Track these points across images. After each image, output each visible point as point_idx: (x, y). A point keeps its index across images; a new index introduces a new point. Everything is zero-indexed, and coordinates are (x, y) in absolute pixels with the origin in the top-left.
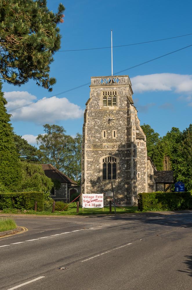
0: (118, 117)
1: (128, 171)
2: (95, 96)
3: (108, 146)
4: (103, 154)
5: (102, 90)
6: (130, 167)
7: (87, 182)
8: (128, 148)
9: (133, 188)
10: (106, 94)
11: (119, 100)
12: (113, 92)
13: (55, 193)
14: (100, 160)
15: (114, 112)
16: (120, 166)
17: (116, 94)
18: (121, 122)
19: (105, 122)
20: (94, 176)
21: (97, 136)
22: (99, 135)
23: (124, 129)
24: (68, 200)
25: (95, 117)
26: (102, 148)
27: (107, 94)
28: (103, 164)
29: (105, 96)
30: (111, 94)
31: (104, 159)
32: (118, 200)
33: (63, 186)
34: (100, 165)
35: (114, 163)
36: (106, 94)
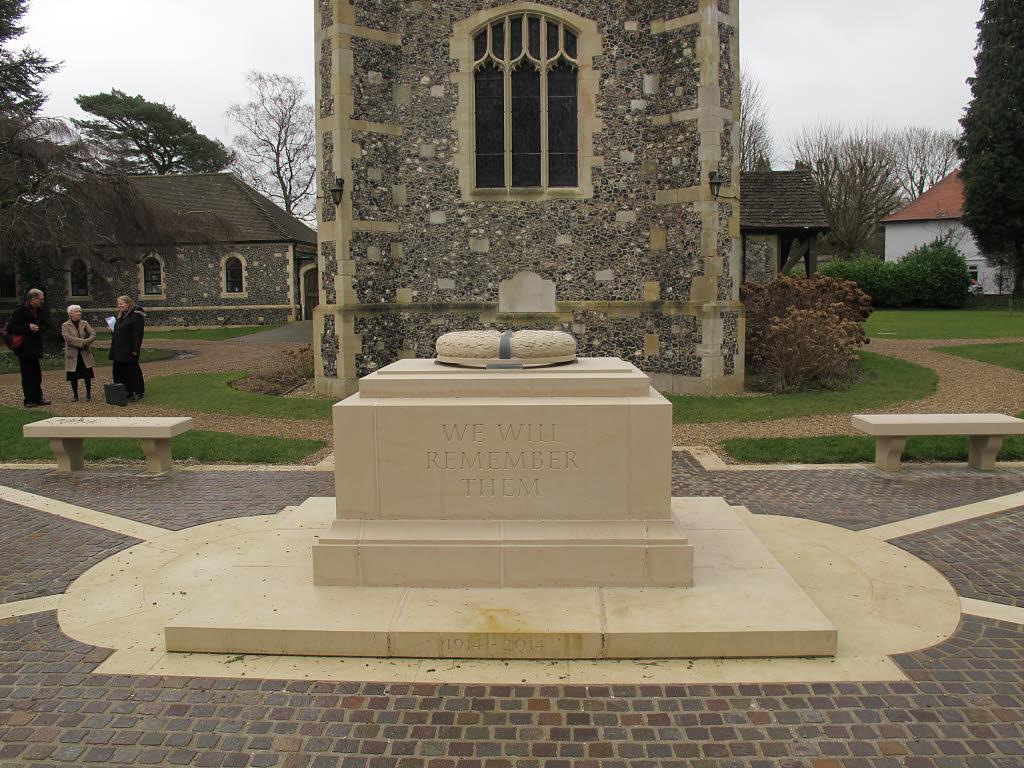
6: (691, 92)
13: (245, 284)
14: (452, 41)
16: (610, 82)
20: (408, 160)
28: (477, 74)
31: (484, 33)
32: (596, 343)
33: (276, 255)
34: (454, 78)
35: (561, 61)
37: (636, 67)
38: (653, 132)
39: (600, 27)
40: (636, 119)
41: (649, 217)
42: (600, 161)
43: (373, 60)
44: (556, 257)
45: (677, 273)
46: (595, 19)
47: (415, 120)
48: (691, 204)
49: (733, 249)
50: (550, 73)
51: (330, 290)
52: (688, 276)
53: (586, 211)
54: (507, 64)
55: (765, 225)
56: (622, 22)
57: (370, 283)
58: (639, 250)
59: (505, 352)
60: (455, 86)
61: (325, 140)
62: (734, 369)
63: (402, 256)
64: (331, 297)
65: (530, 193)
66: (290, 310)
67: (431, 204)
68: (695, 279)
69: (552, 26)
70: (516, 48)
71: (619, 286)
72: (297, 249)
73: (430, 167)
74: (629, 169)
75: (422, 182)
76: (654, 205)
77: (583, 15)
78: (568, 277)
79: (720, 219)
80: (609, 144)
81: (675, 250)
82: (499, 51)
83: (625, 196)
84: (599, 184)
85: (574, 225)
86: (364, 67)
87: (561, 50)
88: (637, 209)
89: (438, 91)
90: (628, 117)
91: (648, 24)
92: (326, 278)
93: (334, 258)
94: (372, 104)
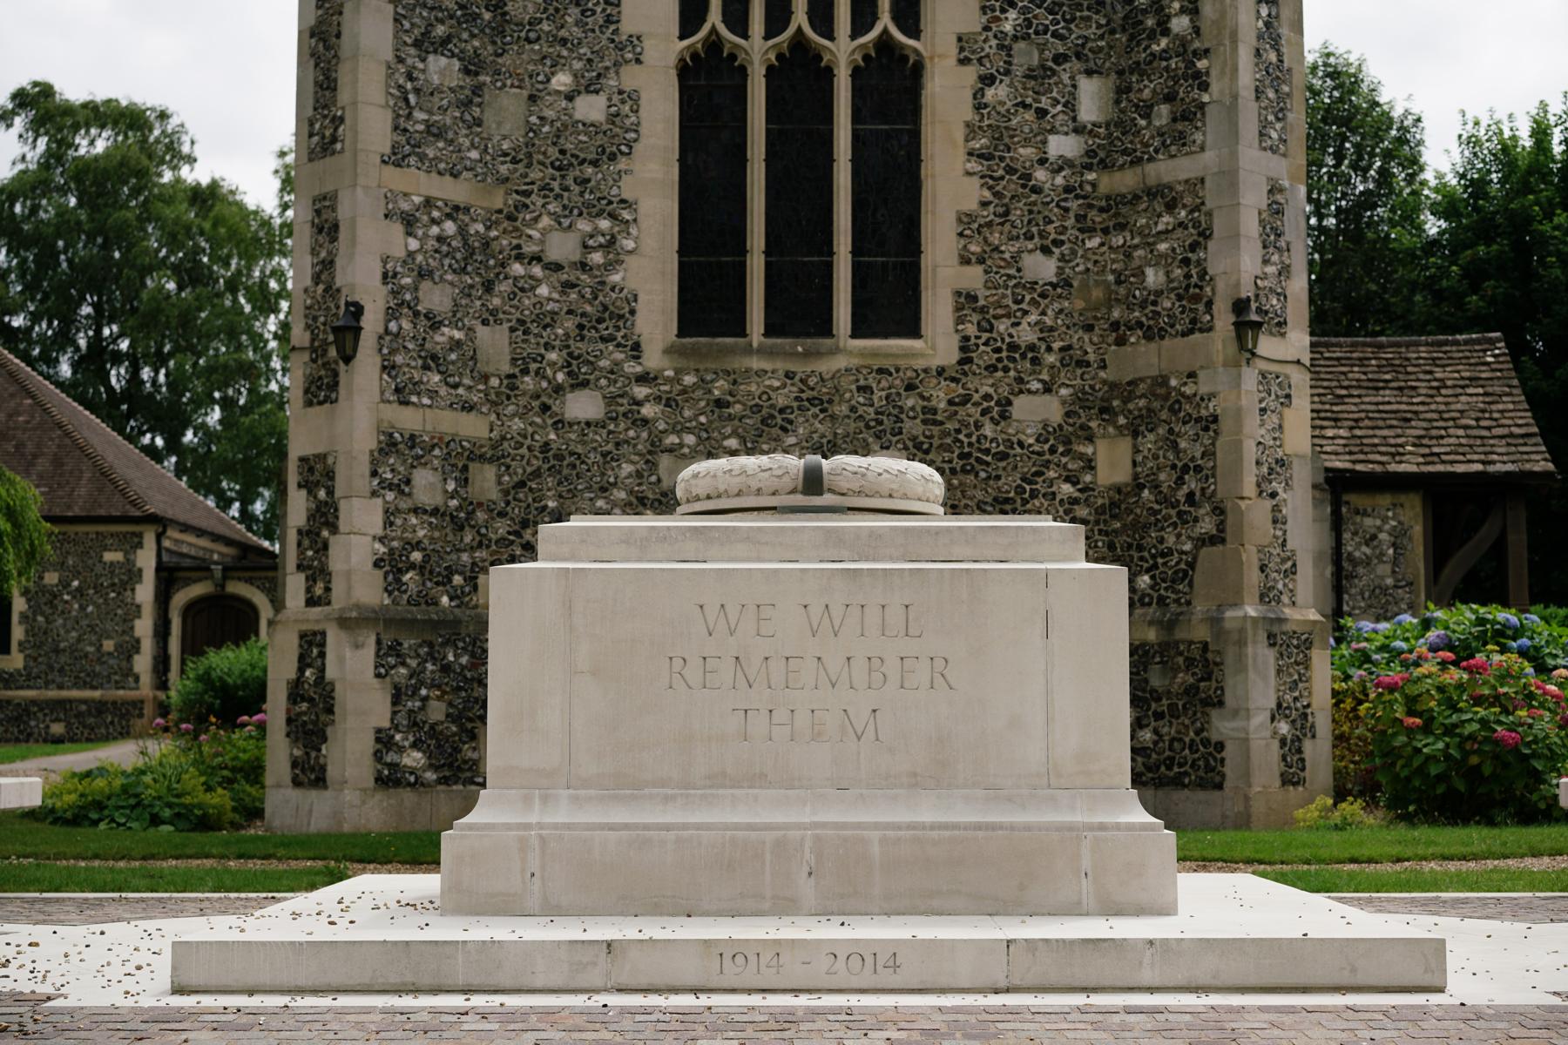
1: (1153, 192)
6: (1190, 115)
7: (388, 368)
9: (1249, 489)
13: (18, 633)
20: (517, 268)
33: (109, 556)
34: (631, 78)
35: (884, 41)
37: (1060, 59)
38: (1102, 210)
40: (1059, 180)
42: (973, 278)
43: (440, 30)
45: (1161, 540)
47: (535, 174)
48: (1192, 375)
49: (1295, 483)
50: (856, 73)
51: (317, 573)
52: (1187, 547)
53: (940, 395)
55: (1393, 467)
57: (416, 556)
58: (1067, 488)
59: (813, 482)
60: (632, 98)
61: (318, 212)
62: (1307, 773)
63: (494, 494)
64: (319, 590)
65: (807, 355)
66: (138, 704)
67: (569, 374)
68: (1204, 551)
72: (166, 543)
73: (569, 285)
74: (1043, 295)
75: (547, 320)
76: (1104, 382)
79: (1263, 411)
80: (995, 238)
81: (1156, 487)
83: (1035, 361)
84: (971, 330)
85: (913, 427)
86: (417, 44)
87: (885, 21)
88: (1063, 391)
89: (591, 108)
90: (1041, 175)
92: (306, 542)
93: (330, 492)
94: (435, 132)
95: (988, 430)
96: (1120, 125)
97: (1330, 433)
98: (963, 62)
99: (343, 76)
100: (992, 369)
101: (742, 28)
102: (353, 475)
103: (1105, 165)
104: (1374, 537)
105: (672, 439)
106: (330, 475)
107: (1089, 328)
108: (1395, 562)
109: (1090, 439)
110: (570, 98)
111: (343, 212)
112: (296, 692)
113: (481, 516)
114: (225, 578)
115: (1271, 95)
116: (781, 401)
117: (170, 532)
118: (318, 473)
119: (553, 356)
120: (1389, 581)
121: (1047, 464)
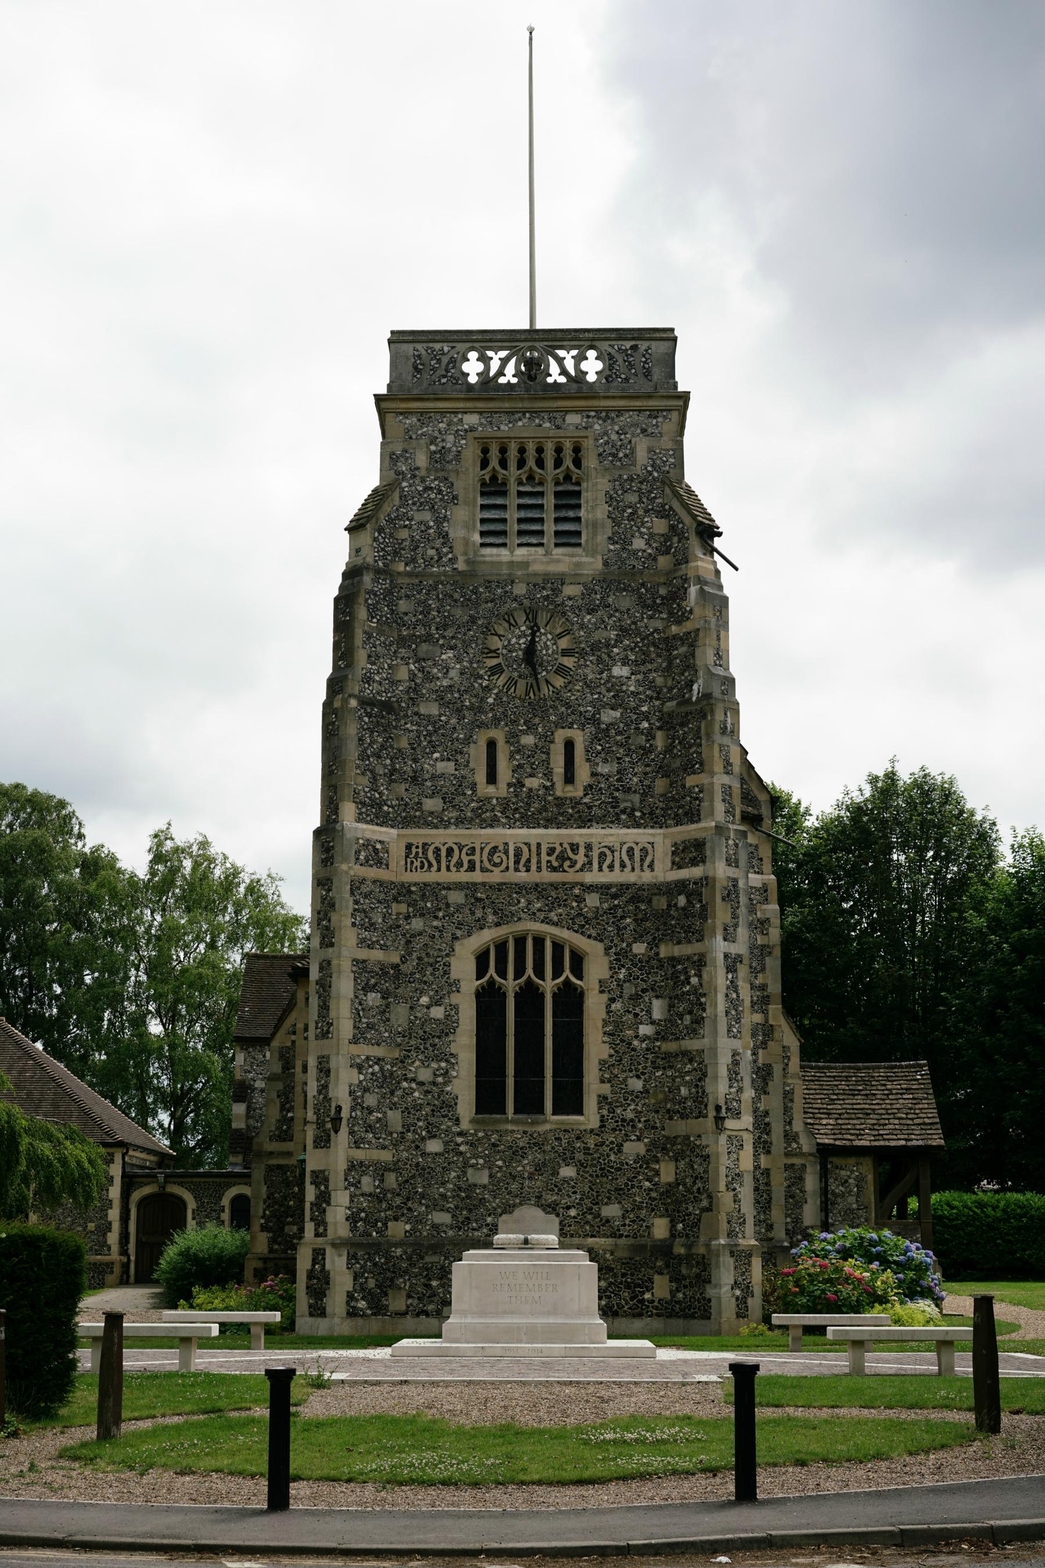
0: (600, 635)
1: (685, 1053)
2: (423, 473)
3: (518, 854)
4: (479, 914)
5: (472, 429)
6: (699, 1021)
7: (352, 1133)
8: (677, 865)
9: (722, 1187)
10: (503, 464)
11: (602, 512)
12: (559, 450)
14: (453, 960)
15: (570, 590)
17: (577, 463)
18: (620, 671)
19: (497, 670)
20: (405, 1084)
21: (434, 777)
22: (448, 767)
23: (646, 725)
24: (126, 1266)
25: (420, 631)
26: (472, 868)
27: (512, 464)
29: (494, 478)
30: (540, 463)
34: (455, 999)
35: (567, 982)
36: (503, 464)
37: (644, 991)
38: (662, 1059)
39: (607, 949)
40: (644, 1045)
41: (661, 1147)
42: (606, 1088)
43: (373, 981)
44: (560, 1190)
45: (687, 1209)
46: (601, 941)
47: (412, 1042)
48: (699, 1136)
49: (745, 1184)
51: (320, 1223)
52: (697, 1212)
53: (591, 1142)
54: (511, 985)
55: (855, 1143)
56: (629, 945)
57: (363, 1215)
58: (647, 1184)
59: (526, 1241)
60: (456, 1008)
61: (320, 1063)
62: (749, 1313)
63: (395, 1186)
64: (321, 1230)
65: (533, 1123)
66: (110, 1265)
67: (428, 1132)
68: (704, 1214)
69: (558, 948)
70: (519, 972)
71: (627, 1222)
73: (427, 1092)
74: (637, 1097)
75: (418, 1108)
76: (664, 1136)
77: (589, 937)
78: (573, 1212)
79: (729, 1153)
80: (616, 1071)
81: (685, 1185)
82: (502, 973)
83: (633, 1126)
84: (605, 1112)
85: (579, 1156)
86: (363, 989)
87: (567, 973)
88: (646, 1140)
89: (438, 1012)
90: (636, 1043)
91: (657, 946)
92: (315, 1209)
93: (327, 1187)
94: (370, 1027)
95: (612, 1157)
96: (670, 1022)
97: (824, 1122)
98: (602, 992)
99: (332, 1004)
100: (614, 1130)
101: (502, 974)
102: (337, 1180)
103: (664, 1039)
104: (846, 1181)
105: (473, 1161)
106: (327, 1180)
107: (657, 1112)
108: (858, 1195)
109: (658, 1162)
110: (428, 1008)
111: (332, 1065)
112: (311, 1275)
113: (389, 1195)
114: (165, 1182)
115: (733, 1012)
116: (521, 1144)
117: (131, 1153)
118: (321, 1178)
119: (421, 1124)
120: (855, 1206)
121: (638, 1173)
